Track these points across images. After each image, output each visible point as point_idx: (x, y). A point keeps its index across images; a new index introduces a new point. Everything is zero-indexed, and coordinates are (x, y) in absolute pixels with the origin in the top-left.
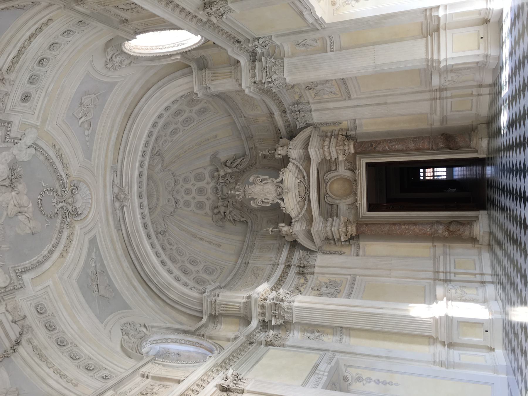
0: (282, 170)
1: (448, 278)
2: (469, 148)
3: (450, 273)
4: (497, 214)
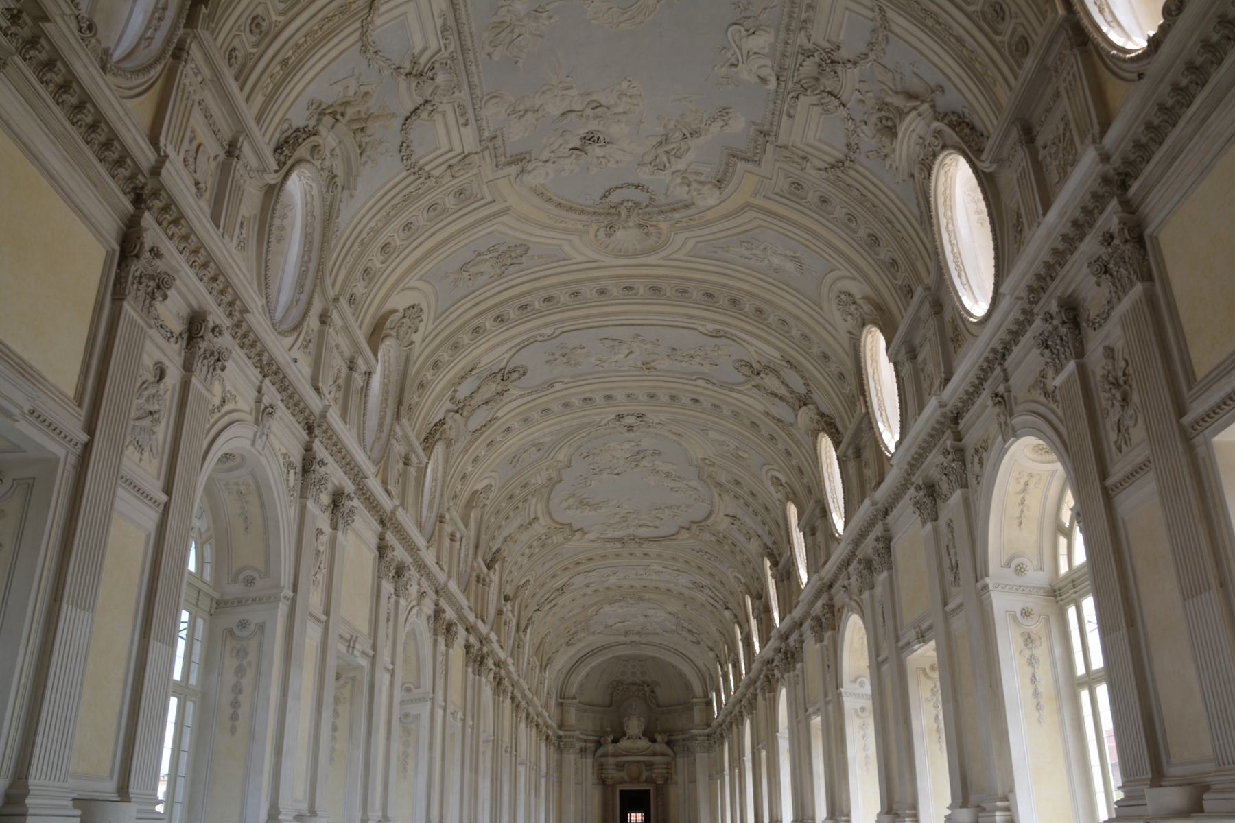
0: (647, 740)
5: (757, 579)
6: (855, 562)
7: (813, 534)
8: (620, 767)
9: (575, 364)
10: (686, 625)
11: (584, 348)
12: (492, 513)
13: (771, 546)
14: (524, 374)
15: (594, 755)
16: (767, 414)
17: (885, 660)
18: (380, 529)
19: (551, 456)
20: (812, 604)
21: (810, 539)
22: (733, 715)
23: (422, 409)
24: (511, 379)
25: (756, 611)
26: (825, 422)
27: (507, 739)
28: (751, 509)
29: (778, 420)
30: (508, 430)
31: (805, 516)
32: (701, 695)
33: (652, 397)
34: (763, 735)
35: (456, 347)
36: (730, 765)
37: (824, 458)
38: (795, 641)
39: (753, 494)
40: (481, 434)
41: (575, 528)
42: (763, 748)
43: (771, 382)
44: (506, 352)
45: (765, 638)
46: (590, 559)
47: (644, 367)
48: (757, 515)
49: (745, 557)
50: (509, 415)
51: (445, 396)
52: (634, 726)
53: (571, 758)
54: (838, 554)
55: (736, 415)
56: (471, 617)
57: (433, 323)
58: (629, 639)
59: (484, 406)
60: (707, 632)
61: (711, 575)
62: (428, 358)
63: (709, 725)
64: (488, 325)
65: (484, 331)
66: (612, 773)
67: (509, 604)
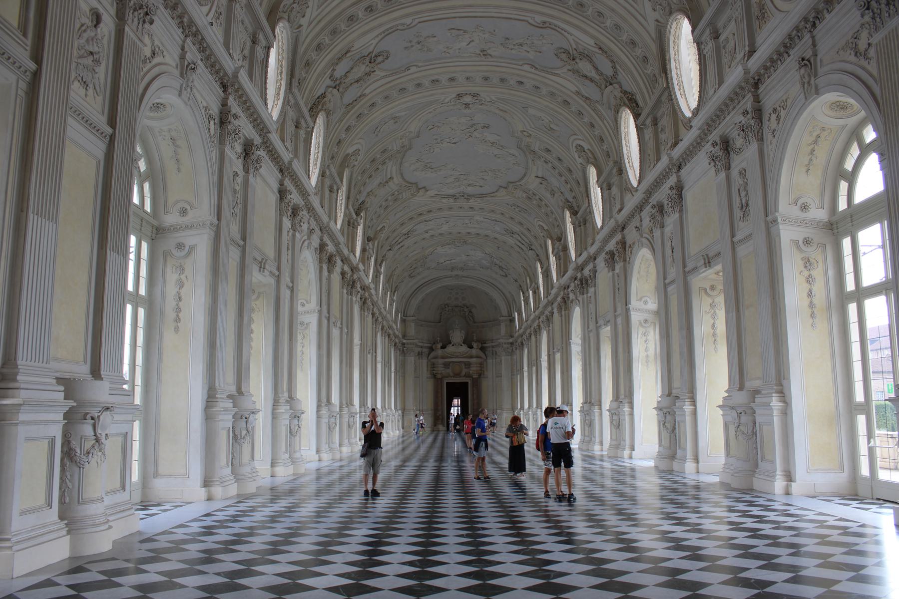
5: (558, 226)
7: (609, 189)
8: (446, 365)
9: (428, 50)
10: (498, 262)
11: (435, 37)
12: (359, 173)
13: (571, 200)
14: (387, 58)
16: (578, 93)
17: (673, 282)
19: (404, 128)
20: (606, 241)
21: (606, 192)
22: (532, 328)
23: (309, 82)
24: (377, 62)
25: (556, 251)
26: (627, 98)
27: (369, 343)
28: (557, 171)
29: (587, 98)
30: (373, 105)
31: (604, 175)
32: (507, 315)
33: (487, 79)
34: (558, 341)
35: (335, 32)
36: (529, 364)
37: (623, 128)
38: (590, 271)
39: (560, 160)
40: (353, 108)
41: (420, 187)
42: (557, 352)
43: (584, 66)
44: (374, 39)
45: (562, 270)
46: (430, 211)
47: (481, 54)
48: (561, 176)
49: (549, 209)
50: (374, 94)
51: (325, 74)
52: (457, 336)
53: (411, 359)
54: (631, 202)
55: (552, 94)
56: (346, 252)
57: (317, 10)
58: (455, 273)
59: (356, 84)
60: (514, 268)
61: (521, 224)
62: (312, 40)
63: (512, 336)
64: (360, 15)
65: (357, 19)
66: (440, 370)
67: (370, 244)
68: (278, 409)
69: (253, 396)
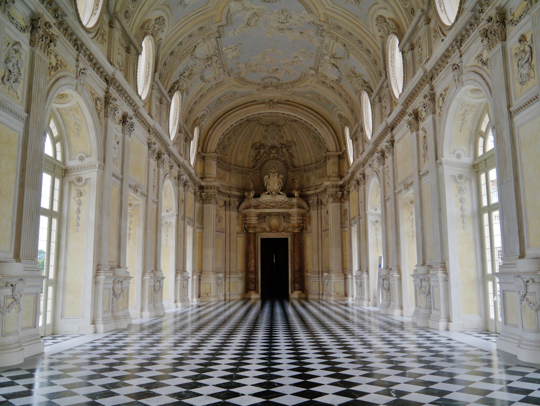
1: (226, 279)
2: (294, 289)
3: (230, 280)
4: (259, 303)
6: (407, 116)
15: (238, 208)
18: (106, 86)
68: (145, 276)
69: (127, 268)
